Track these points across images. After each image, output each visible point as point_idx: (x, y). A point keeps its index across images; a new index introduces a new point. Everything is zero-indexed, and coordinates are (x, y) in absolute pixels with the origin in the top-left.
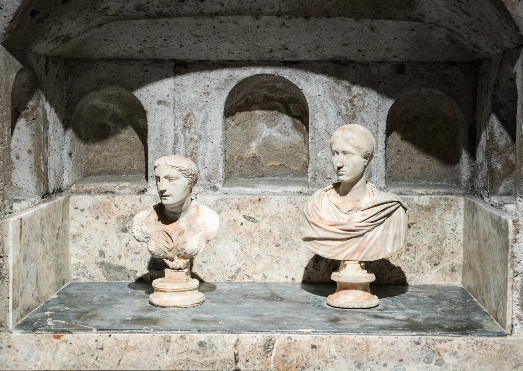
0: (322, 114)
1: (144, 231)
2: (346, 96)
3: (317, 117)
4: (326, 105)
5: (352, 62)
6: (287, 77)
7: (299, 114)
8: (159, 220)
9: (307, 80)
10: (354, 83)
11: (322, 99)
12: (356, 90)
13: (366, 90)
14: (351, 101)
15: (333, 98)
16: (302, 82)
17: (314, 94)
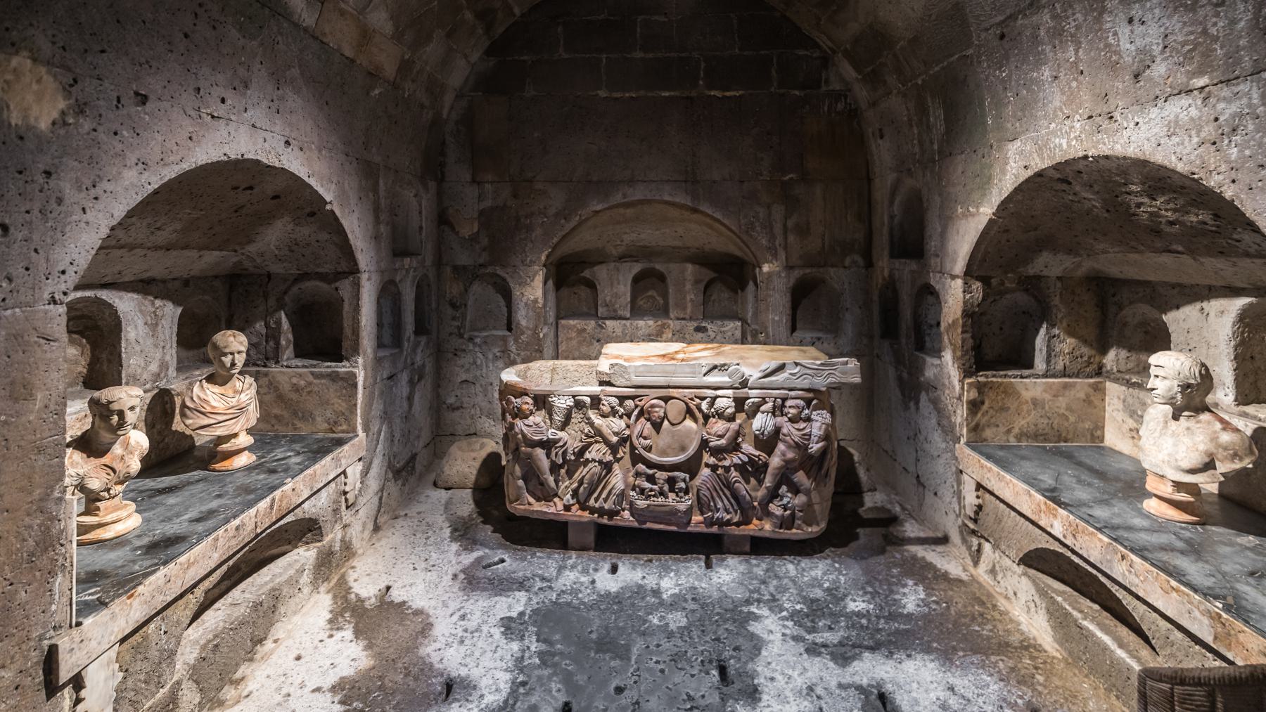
0: (133, 326)
1: (73, 474)
2: (151, 309)
3: (129, 329)
4: (136, 318)
5: (154, 280)
6: (104, 297)
7: (81, 328)
8: (89, 457)
9: (121, 298)
10: (156, 298)
11: (133, 313)
12: (158, 303)
13: (165, 302)
14: (154, 312)
15: (141, 311)
16: (117, 301)
17: (125, 310)
